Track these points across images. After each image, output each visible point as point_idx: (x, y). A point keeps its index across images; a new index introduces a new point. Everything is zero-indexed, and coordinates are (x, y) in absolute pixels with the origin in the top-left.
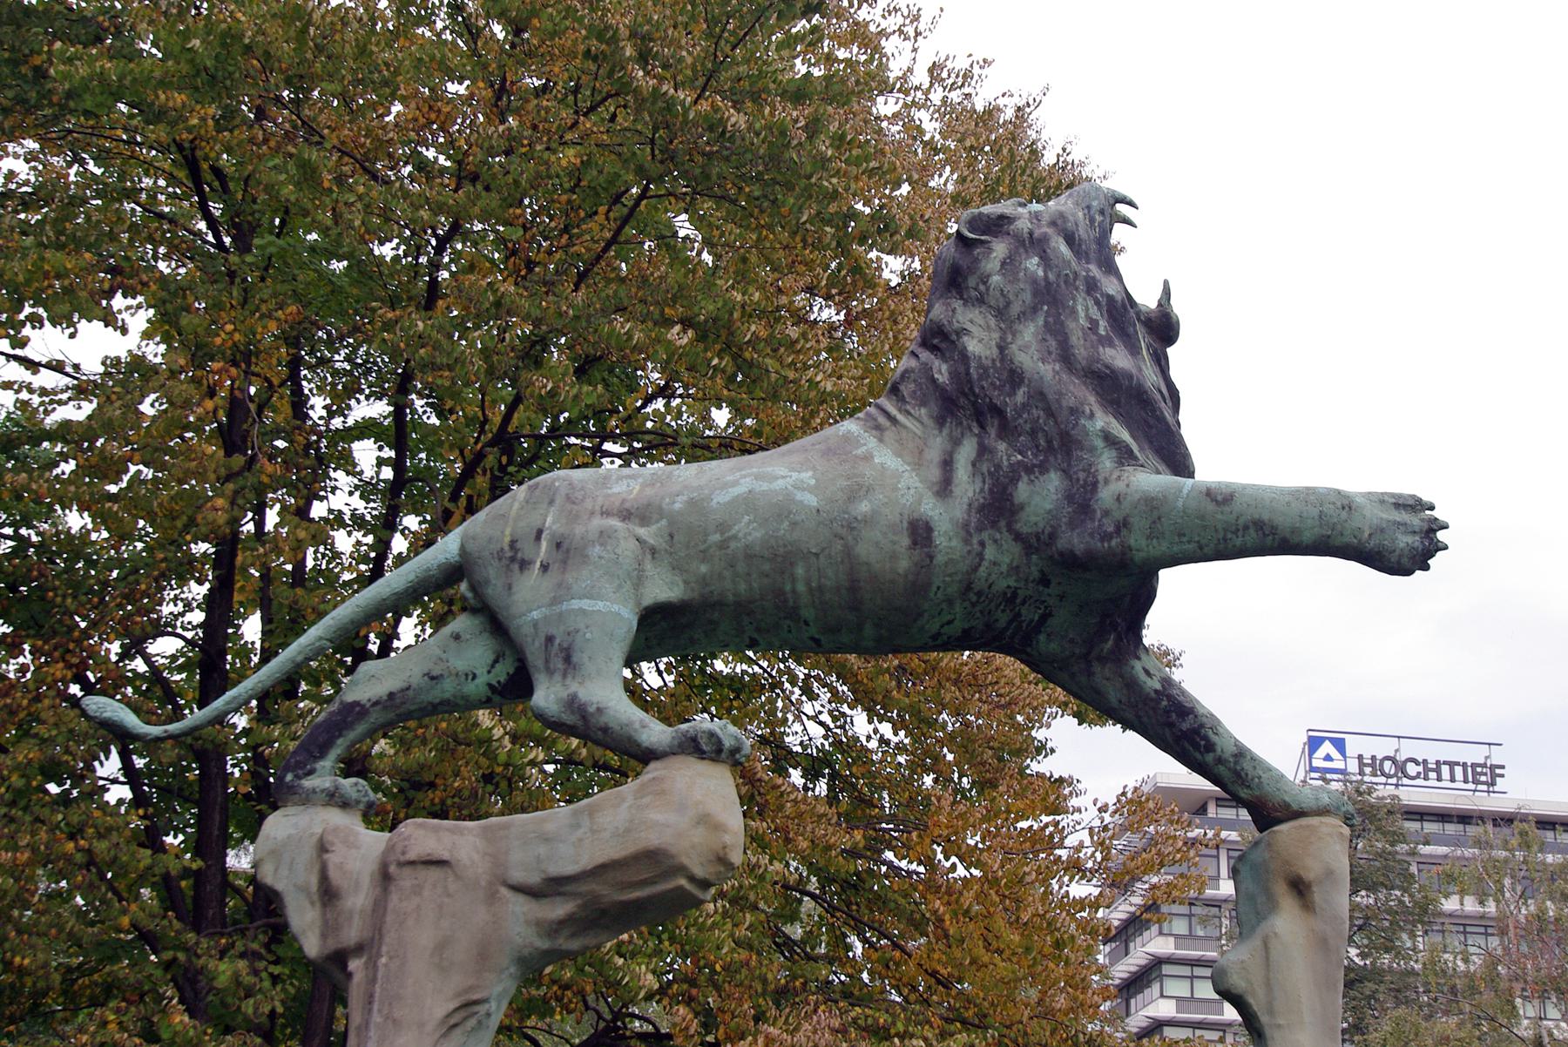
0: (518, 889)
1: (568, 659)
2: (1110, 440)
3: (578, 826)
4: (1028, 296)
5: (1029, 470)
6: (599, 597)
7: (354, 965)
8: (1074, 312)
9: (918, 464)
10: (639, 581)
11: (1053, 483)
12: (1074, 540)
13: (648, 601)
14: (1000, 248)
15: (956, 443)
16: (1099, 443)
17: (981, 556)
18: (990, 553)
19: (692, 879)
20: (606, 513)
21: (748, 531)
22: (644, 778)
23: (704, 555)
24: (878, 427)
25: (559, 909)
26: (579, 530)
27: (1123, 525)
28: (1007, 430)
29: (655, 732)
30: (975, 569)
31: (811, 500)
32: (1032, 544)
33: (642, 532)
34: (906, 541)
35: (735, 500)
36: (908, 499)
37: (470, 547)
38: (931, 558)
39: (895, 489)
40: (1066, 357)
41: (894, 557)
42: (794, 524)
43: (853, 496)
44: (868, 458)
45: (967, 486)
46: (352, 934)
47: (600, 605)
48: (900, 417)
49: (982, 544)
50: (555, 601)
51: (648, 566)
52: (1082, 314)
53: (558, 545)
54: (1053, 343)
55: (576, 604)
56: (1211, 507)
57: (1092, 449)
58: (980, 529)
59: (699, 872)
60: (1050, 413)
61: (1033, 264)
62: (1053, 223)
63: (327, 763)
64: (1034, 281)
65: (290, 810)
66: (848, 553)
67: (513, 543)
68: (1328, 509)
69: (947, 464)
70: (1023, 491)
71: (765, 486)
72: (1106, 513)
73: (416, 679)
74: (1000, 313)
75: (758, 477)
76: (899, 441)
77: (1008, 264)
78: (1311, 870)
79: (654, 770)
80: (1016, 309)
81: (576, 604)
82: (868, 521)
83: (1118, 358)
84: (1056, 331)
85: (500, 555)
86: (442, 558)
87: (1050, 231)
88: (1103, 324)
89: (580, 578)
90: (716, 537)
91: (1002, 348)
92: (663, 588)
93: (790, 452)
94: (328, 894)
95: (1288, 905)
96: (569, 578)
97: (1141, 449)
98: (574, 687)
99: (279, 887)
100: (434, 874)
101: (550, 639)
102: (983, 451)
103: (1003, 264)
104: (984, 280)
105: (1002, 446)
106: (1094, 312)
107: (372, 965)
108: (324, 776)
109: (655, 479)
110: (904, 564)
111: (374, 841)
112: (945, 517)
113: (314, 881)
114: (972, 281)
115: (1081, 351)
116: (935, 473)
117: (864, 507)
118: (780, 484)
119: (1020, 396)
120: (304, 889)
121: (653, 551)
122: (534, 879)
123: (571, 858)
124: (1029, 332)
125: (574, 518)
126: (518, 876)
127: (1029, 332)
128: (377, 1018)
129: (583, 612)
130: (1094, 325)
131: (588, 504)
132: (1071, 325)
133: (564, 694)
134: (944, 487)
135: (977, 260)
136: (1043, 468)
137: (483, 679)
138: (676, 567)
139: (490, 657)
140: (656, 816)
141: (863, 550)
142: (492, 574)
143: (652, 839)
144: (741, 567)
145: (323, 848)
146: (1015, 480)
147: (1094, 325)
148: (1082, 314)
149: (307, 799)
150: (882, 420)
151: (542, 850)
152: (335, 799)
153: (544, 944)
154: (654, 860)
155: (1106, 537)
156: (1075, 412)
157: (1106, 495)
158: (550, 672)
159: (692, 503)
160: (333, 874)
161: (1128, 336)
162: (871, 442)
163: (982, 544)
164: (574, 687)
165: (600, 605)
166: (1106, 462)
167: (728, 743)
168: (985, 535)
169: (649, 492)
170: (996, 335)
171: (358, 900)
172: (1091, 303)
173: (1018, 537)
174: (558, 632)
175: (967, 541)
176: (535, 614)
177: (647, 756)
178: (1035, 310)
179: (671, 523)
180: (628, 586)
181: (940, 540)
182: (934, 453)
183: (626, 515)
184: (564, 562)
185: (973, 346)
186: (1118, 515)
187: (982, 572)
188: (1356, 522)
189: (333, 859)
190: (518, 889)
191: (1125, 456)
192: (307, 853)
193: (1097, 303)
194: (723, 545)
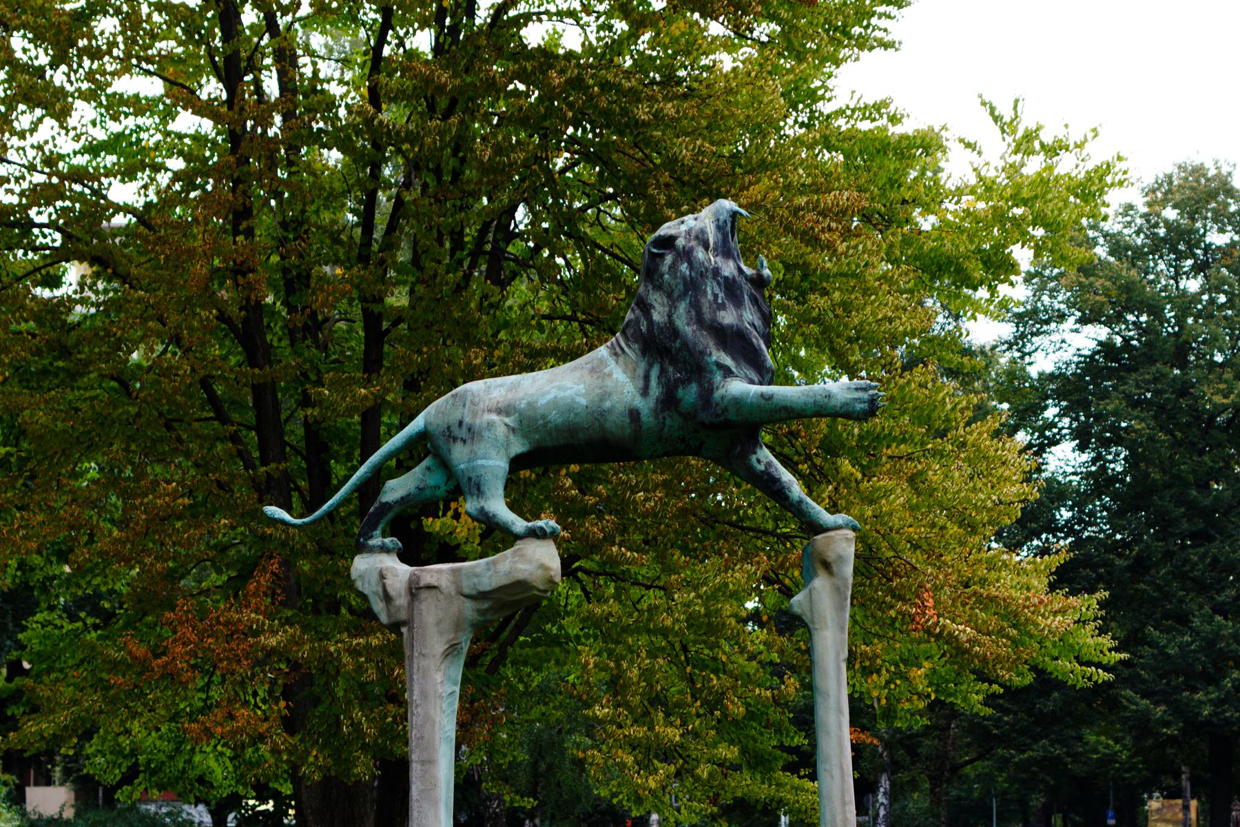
0: (468, 596)
1: (479, 488)
2: (720, 366)
3: (489, 570)
4: (681, 287)
5: (683, 383)
6: (490, 458)
7: (404, 630)
8: (705, 292)
9: (633, 378)
10: (507, 445)
11: (694, 388)
12: (704, 417)
13: (512, 454)
14: (669, 259)
15: (651, 366)
16: (715, 368)
17: (664, 424)
18: (668, 422)
19: (539, 590)
20: (490, 411)
21: (555, 417)
22: (515, 548)
23: (537, 430)
24: (616, 354)
25: (485, 605)
26: (478, 421)
27: (725, 410)
28: (673, 362)
29: (519, 524)
30: (662, 430)
31: (583, 401)
32: (688, 416)
33: (507, 420)
34: (628, 420)
35: (548, 402)
36: (628, 398)
37: (430, 428)
38: (640, 427)
39: (622, 393)
40: (700, 320)
41: (623, 427)
42: (576, 414)
43: (603, 398)
44: (610, 375)
45: (655, 390)
46: (403, 616)
47: (491, 463)
48: (626, 349)
49: (664, 418)
50: (469, 461)
51: (512, 437)
52: (709, 292)
53: (469, 430)
54: (693, 313)
55: (479, 462)
56: (763, 402)
57: (711, 372)
58: (663, 410)
59: (542, 587)
60: (691, 354)
61: (684, 267)
62: (697, 238)
63: (378, 532)
64: (684, 278)
65: (365, 555)
66: (602, 427)
67: (449, 428)
68: (818, 398)
69: (647, 378)
70: (680, 392)
71: (562, 394)
72: (717, 404)
73: (413, 490)
74: (669, 296)
75: (559, 388)
76: (625, 363)
77: (673, 267)
78: (831, 556)
79: (519, 545)
80: (676, 294)
81: (479, 462)
82: (610, 411)
83: (728, 317)
84: (696, 306)
85: (443, 433)
86: (417, 430)
87: (693, 243)
88: (721, 295)
89: (481, 448)
90: (541, 422)
91: (670, 316)
92: (518, 447)
93: (576, 368)
94: (387, 598)
95: (821, 572)
96: (475, 448)
97: (738, 364)
98: (483, 503)
99: (366, 592)
100: (433, 592)
101: (470, 479)
102: (663, 371)
103: (670, 268)
104: (662, 276)
105: (671, 369)
106: (717, 290)
107: (411, 630)
108: (376, 541)
109: (514, 387)
110: (628, 431)
111: (404, 570)
112: (645, 406)
113: (380, 590)
114: (656, 277)
115: (707, 316)
116: (641, 383)
117: (608, 404)
118: (568, 393)
119: (678, 344)
120: (376, 593)
121: (513, 430)
122: (474, 592)
123: (489, 582)
124: (682, 307)
125: (475, 414)
126: (466, 591)
127: (682, 307)
128: (416, 654)
129: (483, 466)
130: (716, 296)
131: (481, 406)
132: (703, 300)
133: (478, 506)
134: (645, 392)
135: (657, 265)
136: (690, 382)
137: (443, 489)
138: (525, 436)
139: (445, 479)
140: (521, 566)
141: (608, 425)
142: (441, 442)
143: (520, 576)
144: (554, 434)
145: (382, 577)
146: (676, 387)
147: (716, 296)
148: (709, 292)
149: (371, 550)
150: (618, 350)
151: (476, 580)
152: (384, 549)
153: (482, 619)
154: (521, 585)
155: (718, 416)
156: (702, 353)
157: (717, 395)
158: (472, 495)
159: (529, 404)
160: (389, 589)
161: (736, 297)
162: (612, 363)
163: (664, 418)
164: (483, 503)
165: (491, 463)
166: (718, 377)
167: (548, 530)
168: (665, 414)
169: (510, 396)
170: (667, 309)
171: (402, 601)
172: (715, 284)
173: (680, 414)
174: (473, 475)
175: (656, 417)
176: (462, 466)
177: (518, 537)
178: (685, 294)
179: (520, 415)
180: (503, 450)
181: (644, 418)
182: (641, 372)
183: (499, 411)
184: (473, 439)
185: (656, 317)
186: (722, 405)
187: (666, 429)
188: (833, 402)
189: (388, 582)
190: (468, 596)
191: (728, 372)
192: (375, 578)
193: (719, 283)
194: (545, 425)
